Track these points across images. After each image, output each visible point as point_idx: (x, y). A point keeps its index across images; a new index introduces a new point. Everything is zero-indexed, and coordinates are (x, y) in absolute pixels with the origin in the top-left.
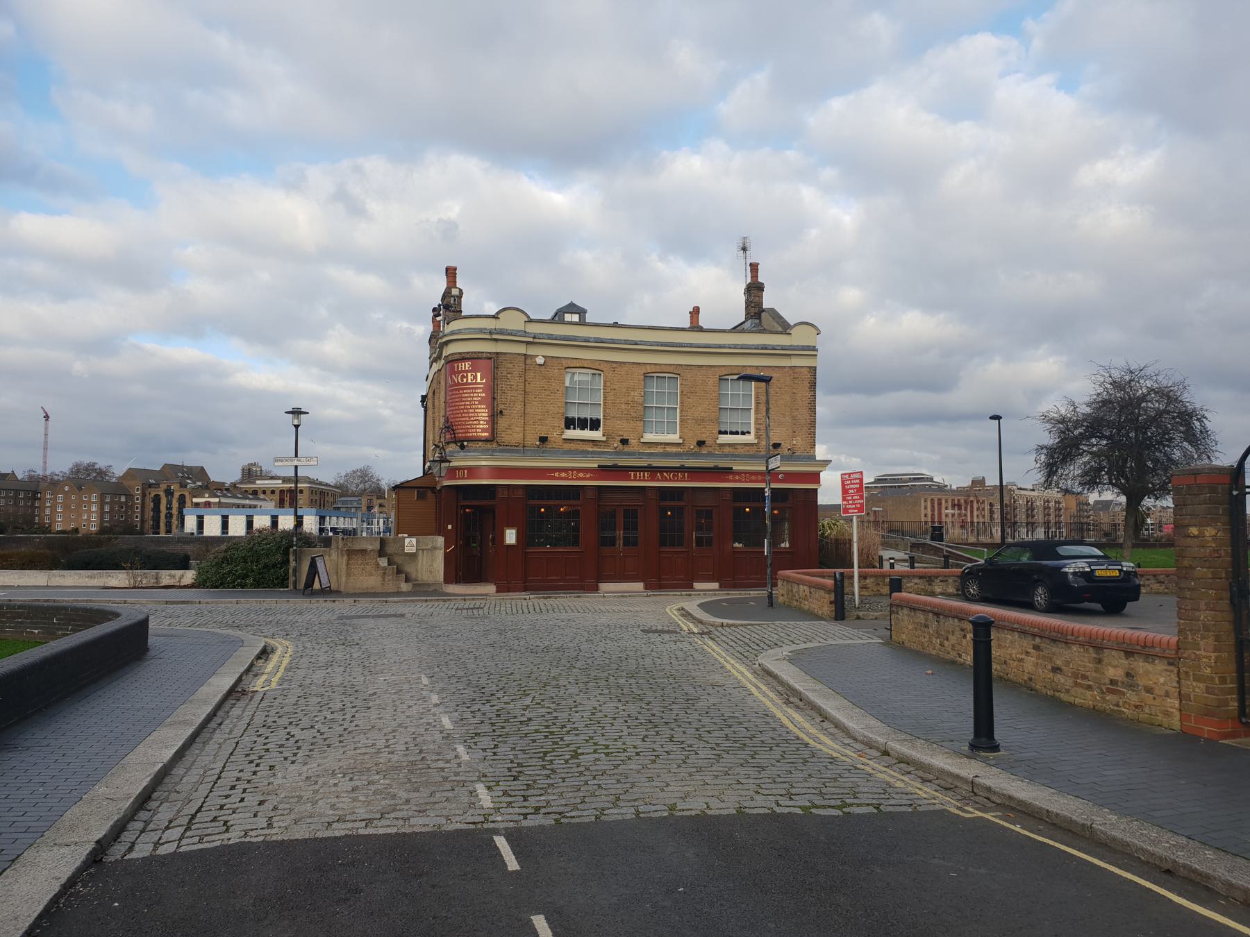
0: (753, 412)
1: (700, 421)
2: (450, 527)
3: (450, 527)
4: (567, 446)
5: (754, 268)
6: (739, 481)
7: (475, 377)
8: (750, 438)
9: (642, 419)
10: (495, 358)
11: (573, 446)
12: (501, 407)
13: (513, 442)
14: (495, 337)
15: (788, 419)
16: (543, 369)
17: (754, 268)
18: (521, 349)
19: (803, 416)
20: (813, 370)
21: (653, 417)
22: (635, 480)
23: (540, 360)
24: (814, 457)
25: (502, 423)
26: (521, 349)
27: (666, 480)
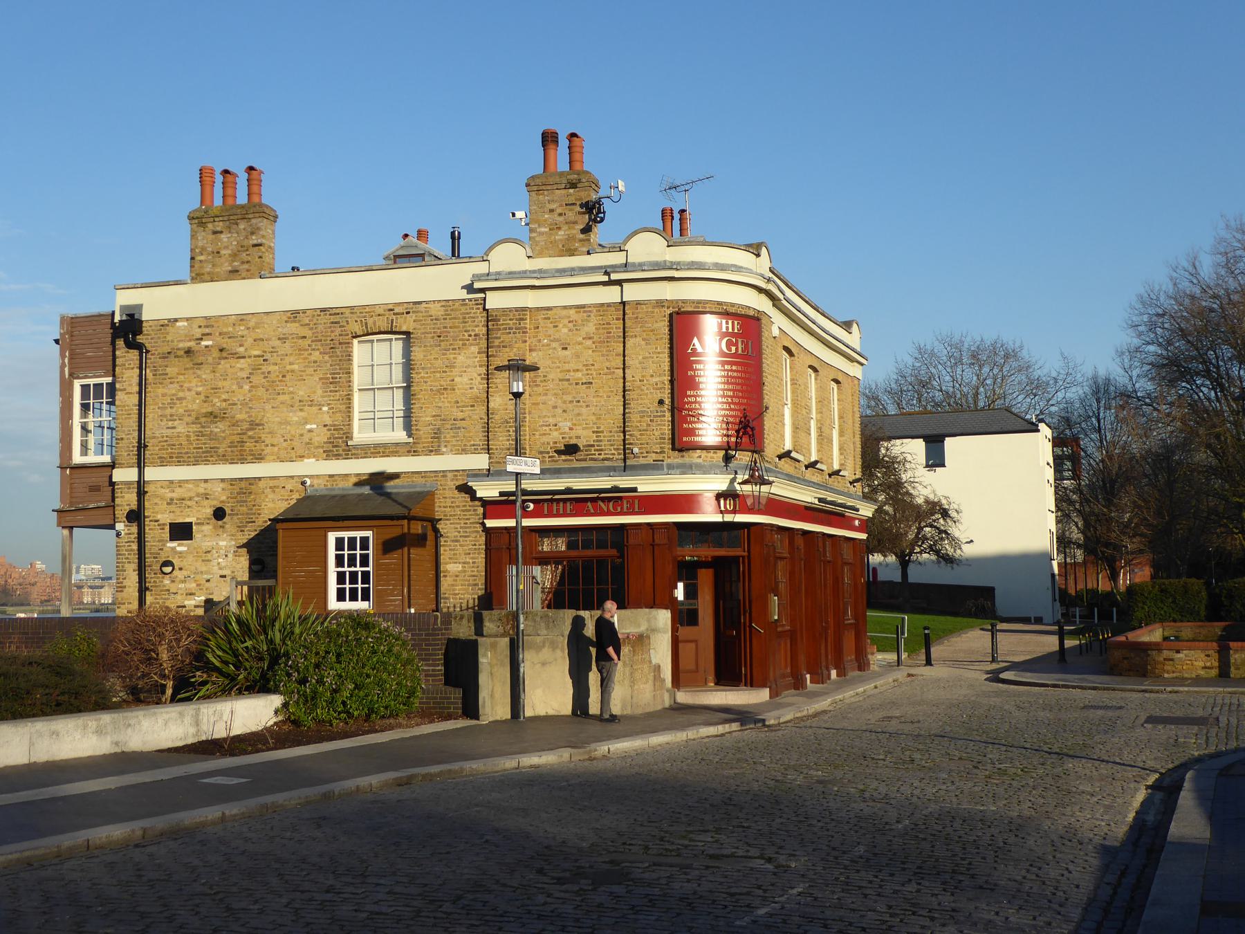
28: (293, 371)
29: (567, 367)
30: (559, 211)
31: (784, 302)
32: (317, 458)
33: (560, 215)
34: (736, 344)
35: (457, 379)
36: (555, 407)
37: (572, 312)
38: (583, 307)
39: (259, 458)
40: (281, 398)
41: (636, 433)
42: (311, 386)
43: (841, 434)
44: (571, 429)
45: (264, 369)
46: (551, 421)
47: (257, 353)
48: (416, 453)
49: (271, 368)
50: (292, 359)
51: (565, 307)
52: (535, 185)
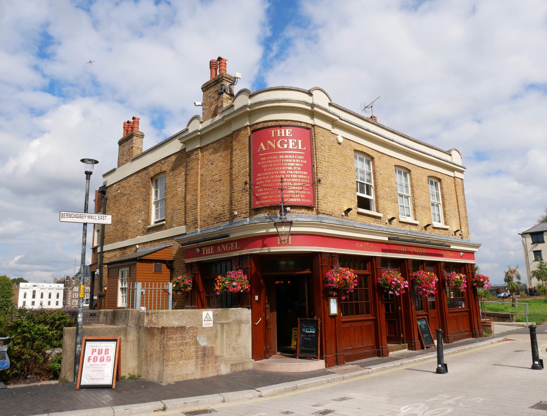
0: (441, 207)
7: (297, 144)
12: (320, 176)
13: (328, 211)
14: (315, 109)
23: (341, 140)
25: (321, 190)
28: (136, 198)
29: (213, 173)
30: (212, 96)
31: (340, 121)
32: (140, 235)
33: (213, 98)
34: (288, 143)
35: (178, 189)
36: (208, 196)
37: (215, 144)
38: (219, 140)
39: (127, 238)
40: (133, 210)
41: (236, 203)
42: (139, 205)
43: (444, 206)
44: (214, 206)
45: (130, 198)
46: (207, 203)
47: (128, 192)
48: (166, 229)
49: (131, 198)
50: (135, 193)
51: (213, 143)
52: (206, 88)
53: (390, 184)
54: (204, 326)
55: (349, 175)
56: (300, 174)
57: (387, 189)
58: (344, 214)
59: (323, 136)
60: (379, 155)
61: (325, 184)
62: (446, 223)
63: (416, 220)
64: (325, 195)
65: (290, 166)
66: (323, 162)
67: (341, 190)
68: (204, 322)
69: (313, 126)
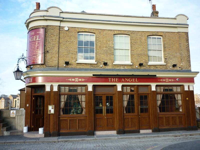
0: (162, 51)
1: (139, 55)
2: (28, 105)
3: (28, 105)
4: (79, 67)
5: (154, 7)
6: (165, 82)
8: (163, 63)
9: (113, 54)
10: (46, 28)
11: (81, 67)
12: (48, 49)
13: (53, 65)
15: (178, 54)
16: (67, 32)
17: (154, 7)
18: (57, 24)
19: (184, 53)
20: (187, 34)
21: (117, 53)
22: (111, 82)
24: (191, 70)
25: (48, 56)
26: (57, 24)
27: (127, 82)
53: (107, 45)
54: (11, 116)
55: (71, 45)
56: (36, 51)
57: (104, 48)
58: (65, 65)
59: (53, 30)
60: (100, 31)
61: (52, 53)
62: (165, 62)
63: (131, 62)
64: (52, 58)
65: (33, 48)
66: (52, 42)
67: (65, 53)
68: (11, 115)
69: (47, 26)
